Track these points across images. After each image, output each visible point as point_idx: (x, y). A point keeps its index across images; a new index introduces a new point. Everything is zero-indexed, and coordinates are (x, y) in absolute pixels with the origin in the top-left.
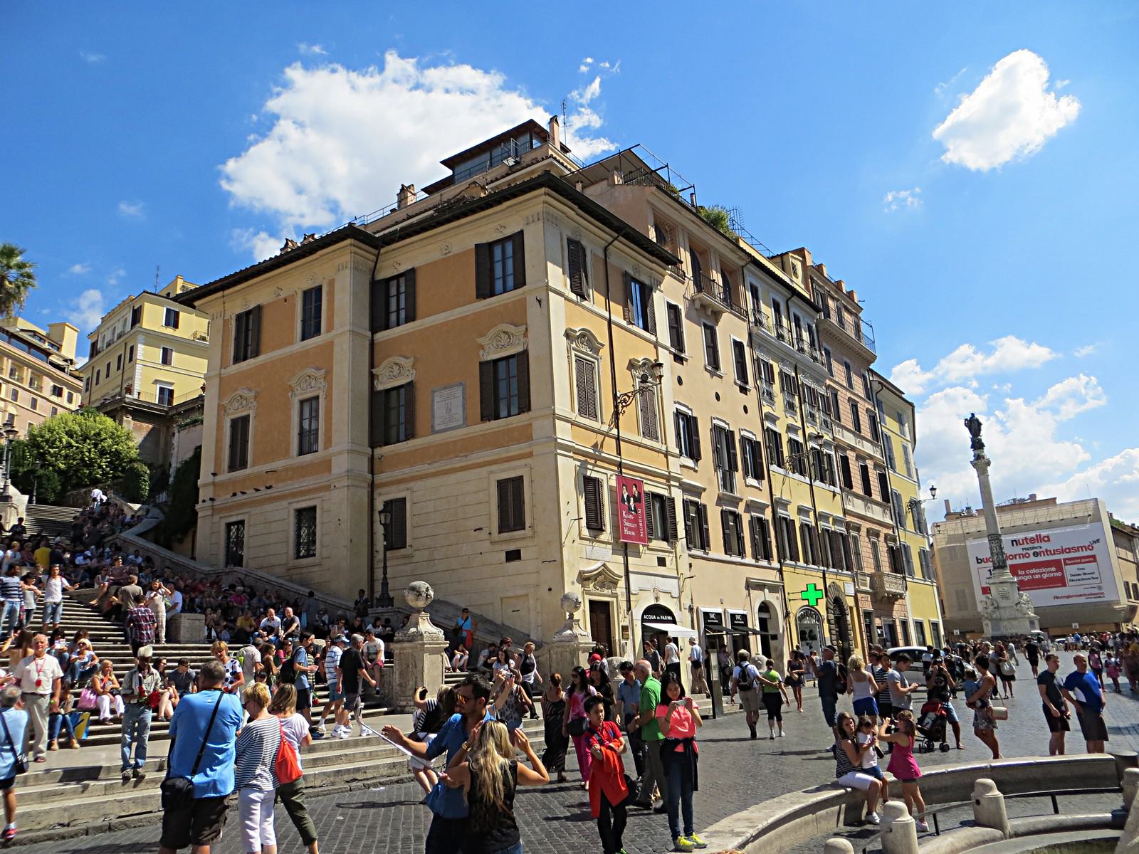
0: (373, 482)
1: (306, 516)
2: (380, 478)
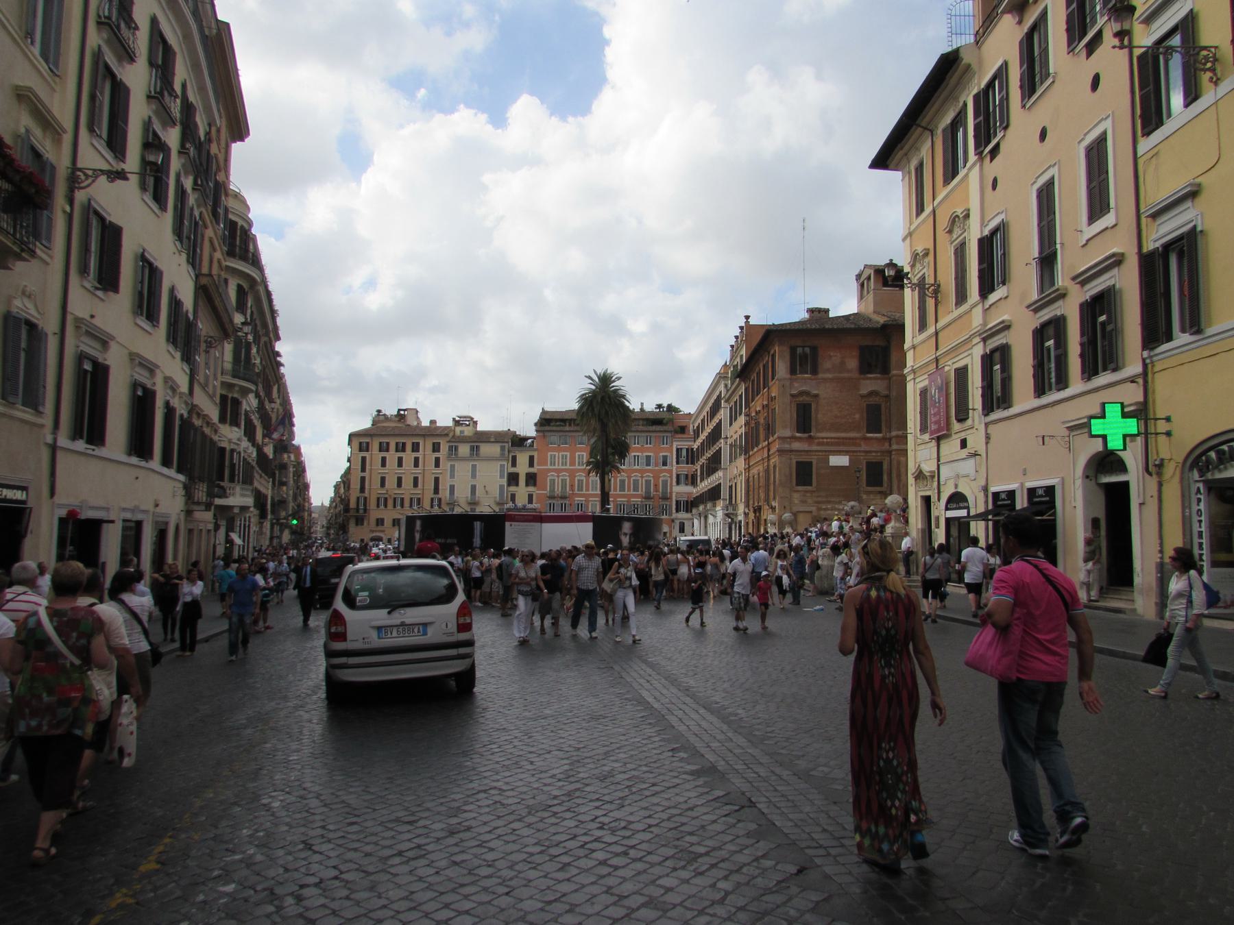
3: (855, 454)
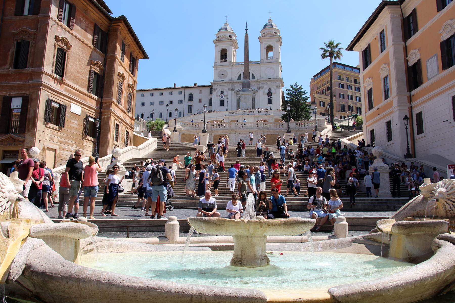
0: (411, 106)
1: (389, 124)
2: (413, 104)
3: (84, 107)
